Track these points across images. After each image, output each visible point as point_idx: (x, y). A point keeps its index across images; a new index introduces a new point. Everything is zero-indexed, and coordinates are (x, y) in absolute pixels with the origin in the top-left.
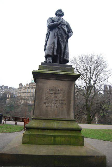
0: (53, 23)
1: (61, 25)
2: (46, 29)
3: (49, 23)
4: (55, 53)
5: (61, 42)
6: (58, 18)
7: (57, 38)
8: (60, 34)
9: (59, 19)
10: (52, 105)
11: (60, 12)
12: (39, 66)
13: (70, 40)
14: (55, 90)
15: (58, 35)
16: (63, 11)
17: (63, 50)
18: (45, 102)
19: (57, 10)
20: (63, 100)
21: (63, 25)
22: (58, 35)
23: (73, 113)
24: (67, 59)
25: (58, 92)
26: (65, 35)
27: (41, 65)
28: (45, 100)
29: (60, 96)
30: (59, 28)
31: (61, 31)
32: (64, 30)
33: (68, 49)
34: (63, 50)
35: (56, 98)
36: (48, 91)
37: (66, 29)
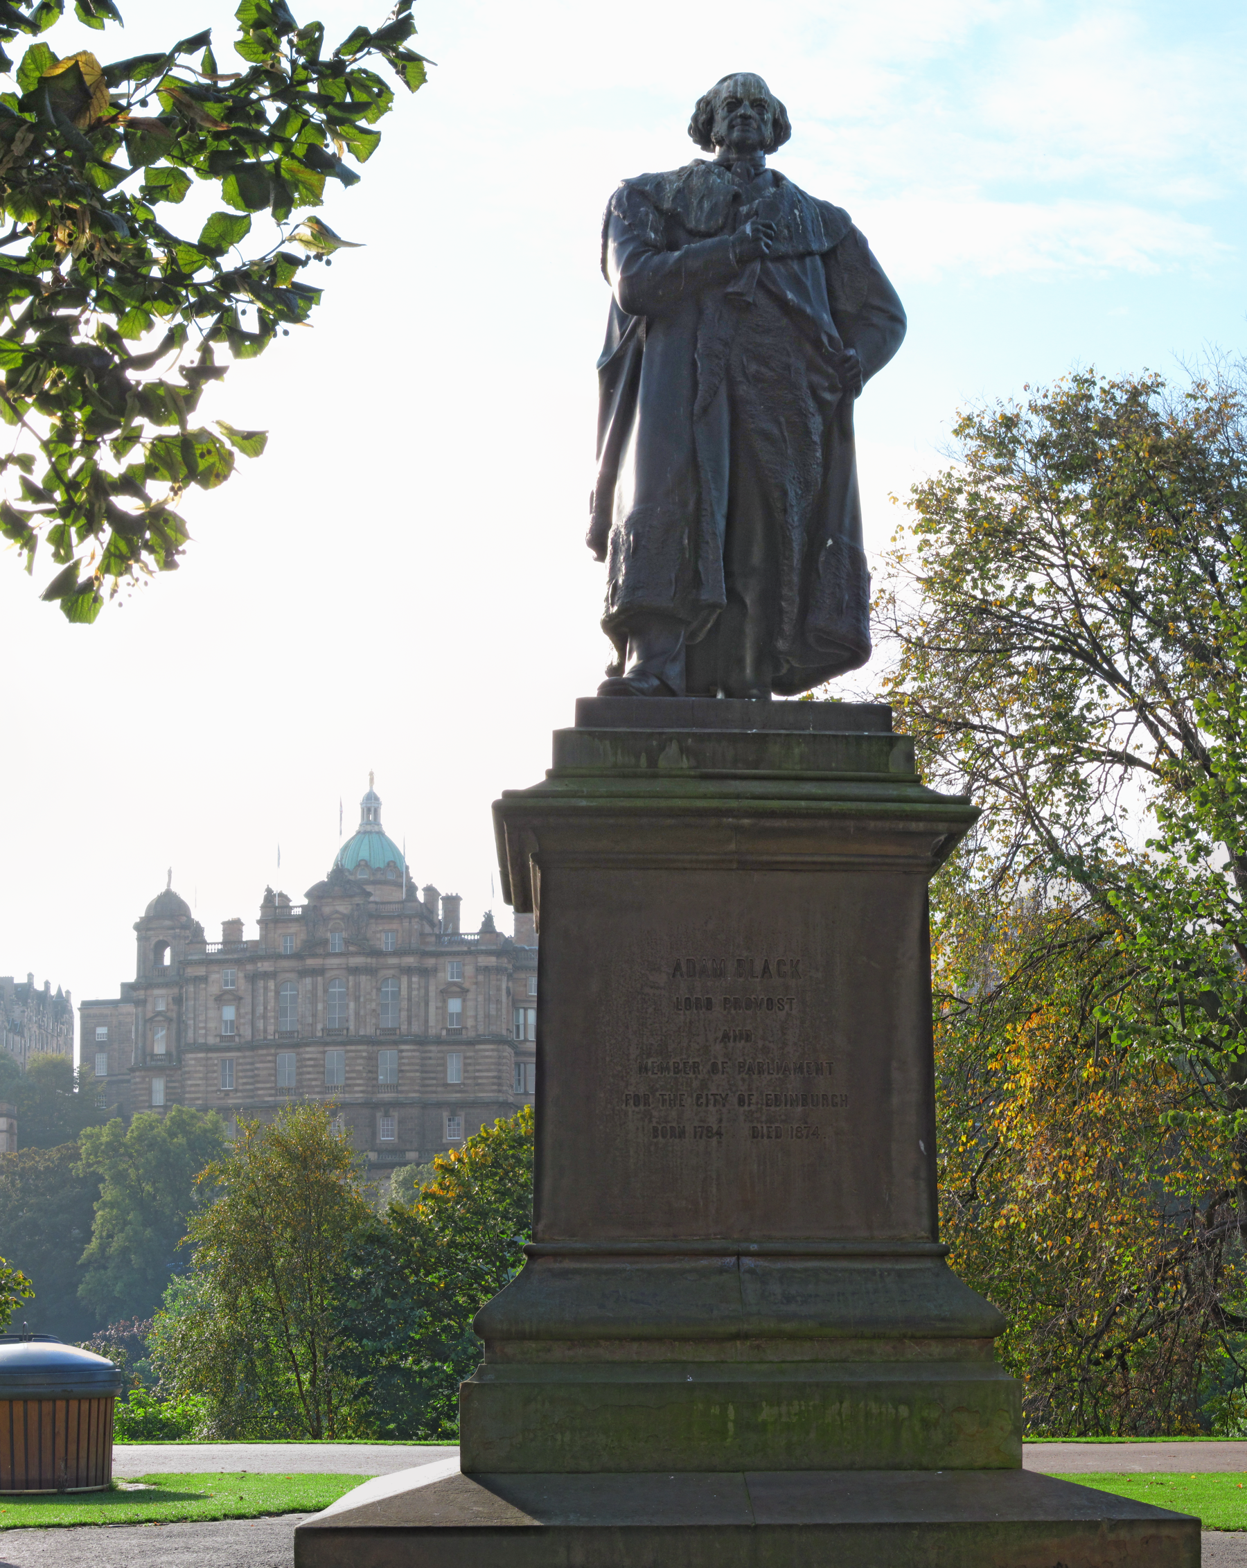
1: (757, 267)
8: (753, 368)
10: (712, 1122)
15: (732, 384)
16: (777, 89)
22: (732, 384)
26: (811, 367)
28: (643, 1069)
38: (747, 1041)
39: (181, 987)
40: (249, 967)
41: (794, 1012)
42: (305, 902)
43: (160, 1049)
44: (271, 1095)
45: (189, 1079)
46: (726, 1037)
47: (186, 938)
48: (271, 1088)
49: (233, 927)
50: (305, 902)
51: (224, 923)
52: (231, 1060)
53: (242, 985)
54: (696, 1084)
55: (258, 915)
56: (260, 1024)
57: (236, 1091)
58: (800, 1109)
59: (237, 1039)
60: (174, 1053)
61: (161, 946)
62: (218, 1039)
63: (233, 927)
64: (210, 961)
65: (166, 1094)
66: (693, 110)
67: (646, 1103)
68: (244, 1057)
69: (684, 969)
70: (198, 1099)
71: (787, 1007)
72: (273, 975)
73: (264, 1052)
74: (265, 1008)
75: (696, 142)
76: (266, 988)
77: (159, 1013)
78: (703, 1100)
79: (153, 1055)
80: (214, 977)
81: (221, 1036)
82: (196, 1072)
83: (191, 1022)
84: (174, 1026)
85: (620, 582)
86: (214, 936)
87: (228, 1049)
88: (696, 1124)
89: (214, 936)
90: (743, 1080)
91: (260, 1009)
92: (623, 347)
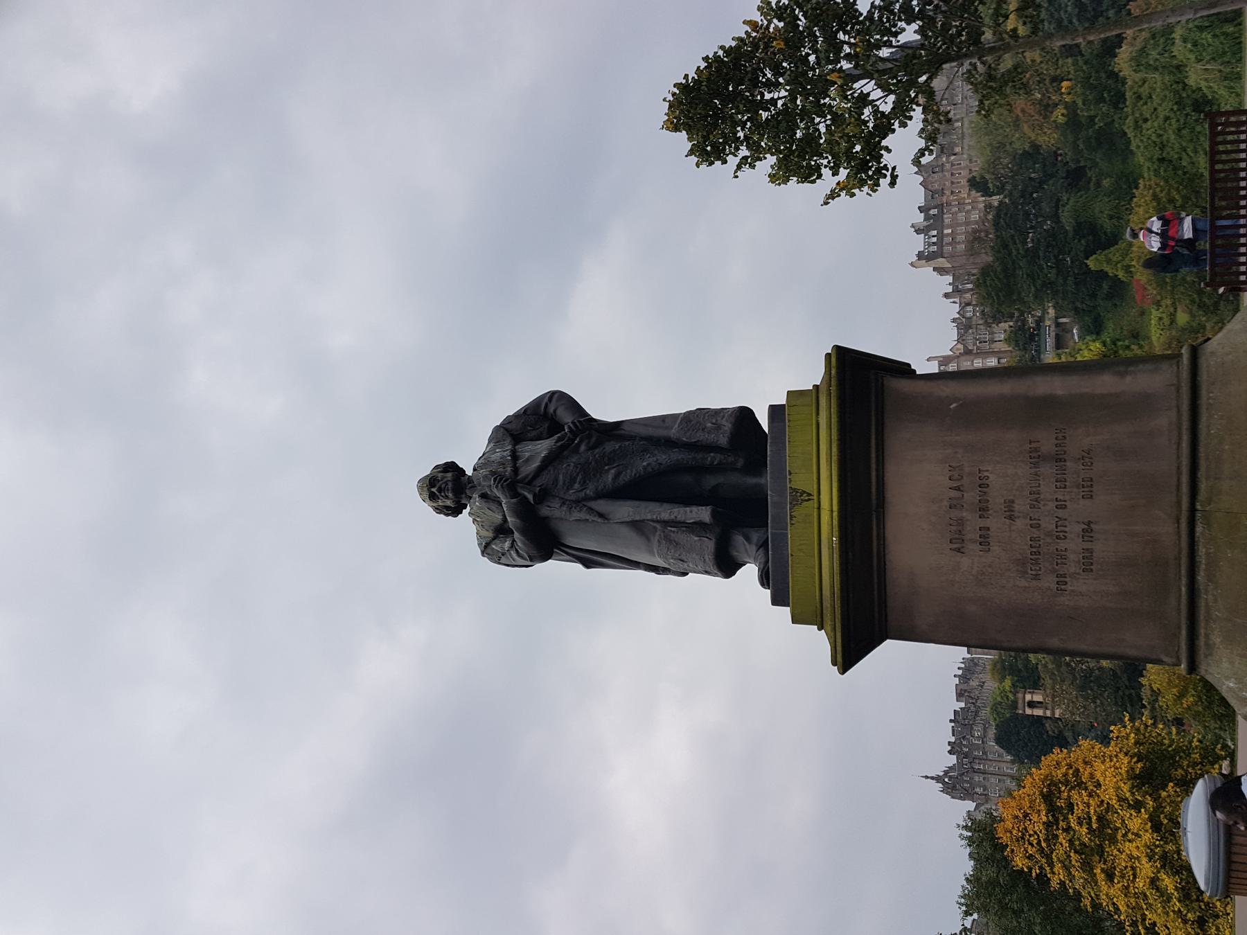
0: (516, 535)
2: (558, 572)
3: (514, 555)
4: (703, 514)
5: (626, 477)
6: (477, 501)
7: (601, 505)
8: (577, 486)
9: (484, 496)
10: (1079, 528)
11: (440, 490)
12: (796, 620)
13: (603, 409)
14: (955, 514)
15: (587, 498)
16: (427, 471)
17: (676, 456)
19: (426, 509)
20: (1036, 458)
21: (516, 470)
22: (587, 498)
23: (1132, 368)
24: (727, 426)
25: (971, 496)
27: (786, 611)
28: (1036, 577)
29: (1006, 476)
30: (543, 495)
31: (556, 480)
32: (548, 462)
33: (663, 418)
34: (676, 456)
35: (1021, 506)
36: (965, 562)
37: (542, 448)
38: (1013, 502)
46: (1011, 518)
54: (1048, 540)
58: (1068, 463)
67: (1064, 576)
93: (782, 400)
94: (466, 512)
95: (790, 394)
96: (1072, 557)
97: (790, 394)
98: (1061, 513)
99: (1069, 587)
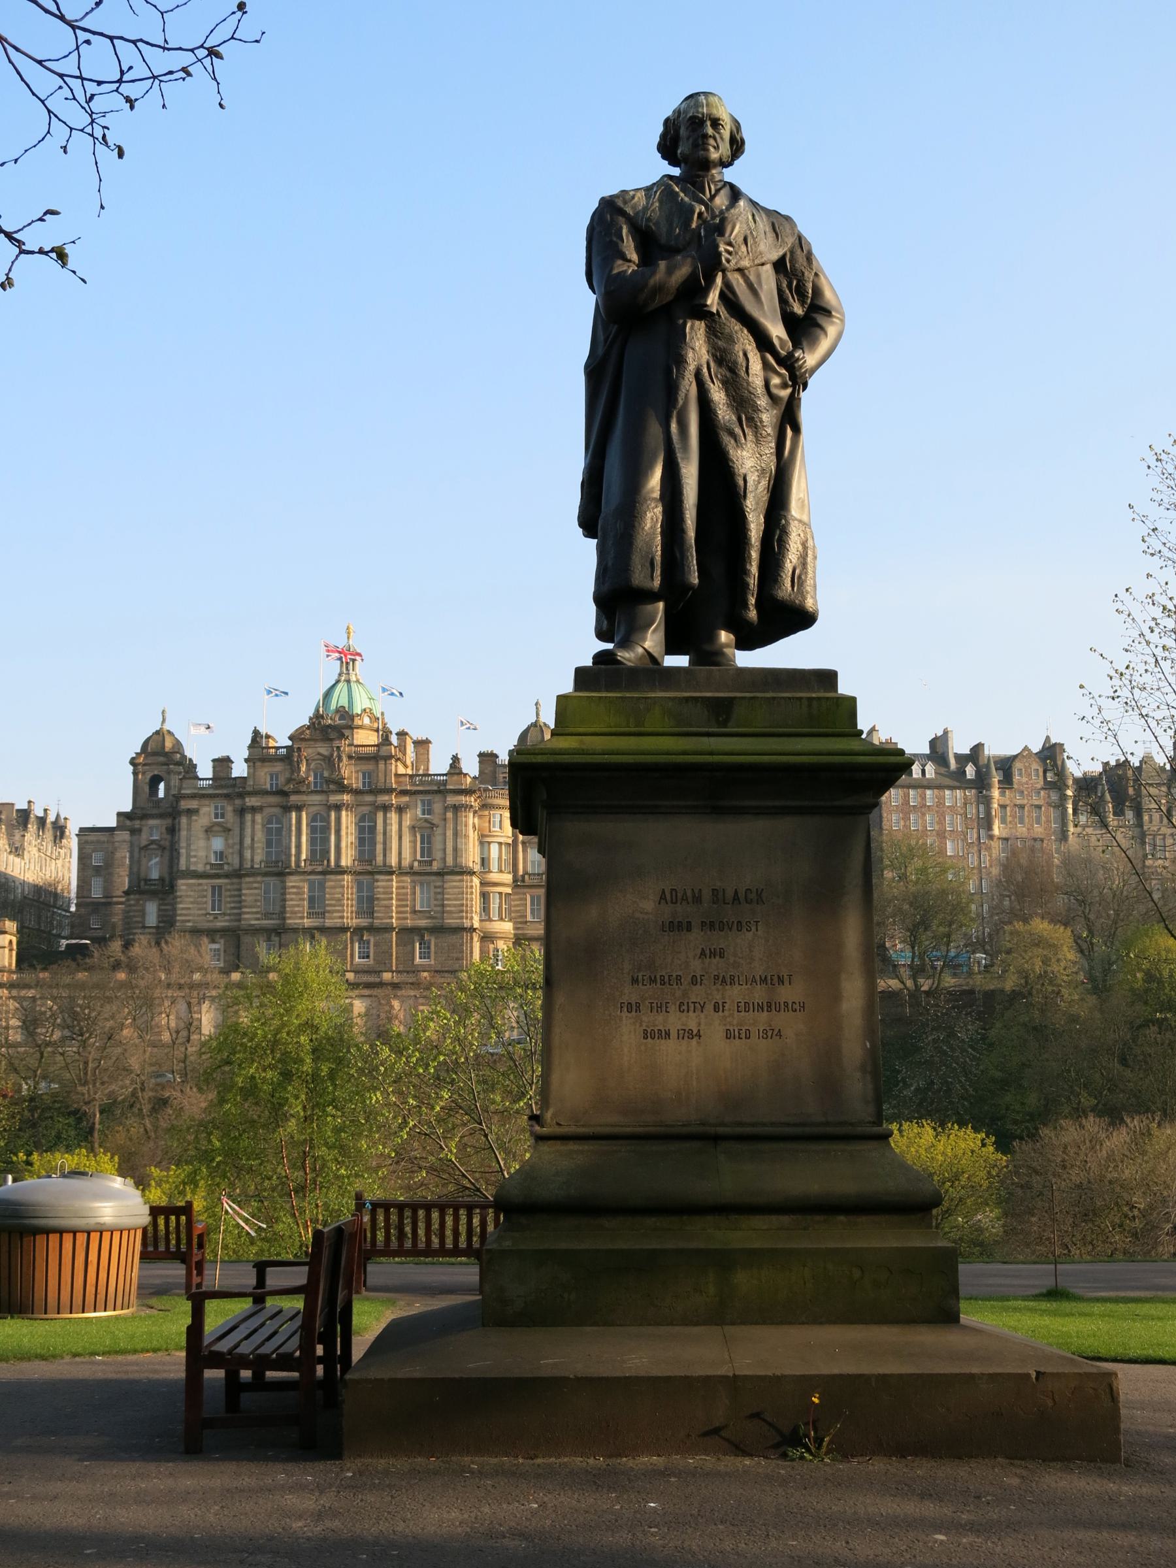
18: (634, 999)
23: (868, 1077)
39: (174, 818)
40: (238, 802)
41: (759, 933)
42: (290, 743)
43: (155, 875)
44: (258, 919)
45: (181, 903)
47: (180, 773)
48: (257, 913)
49: (223, 764)
50: (290, 743)
51: (214, 761)
52: (220, 887)
53: (230, 818)
54: (678, 993)
55: (246, 754)
56: (248, 854)
57: (224, 914)
58: (765, 1013)
59: (226, 867)
60: (167, 880)
61: (155, 781)
62: (208, 867)
63: (223, 764)
64: (201, 796)
65: (159, 916)
66: (660, 129)
67: (638, 1009)
68: (232, 884)
69: (668, 898)
70: (189, 921)
71: (753, 928)
72: (260, 809)
73: (251, 879)
74: (253, 839)
75: (664, 157)
76: (253, 821)
77: (153, 842)
78: (685, 1007)
79: (147, 881)
80: (204, 810)
81: (212, 865)
82: (187, 896)
83: (183, 851)
84: (167, 853)
85: (610, 564)
86: (205, 771)
87: (217, 876)
88: (680, 1027)
89: (205, 771)
90: (718, 990)
91: (248, 841)
92: (607, 354)
93: (844, 688)
94: (666, 169)
95: (852, 701)
96: (660, 1018)
97: (852, 701)
98: (709, 1007)
99: (625, 1014)
